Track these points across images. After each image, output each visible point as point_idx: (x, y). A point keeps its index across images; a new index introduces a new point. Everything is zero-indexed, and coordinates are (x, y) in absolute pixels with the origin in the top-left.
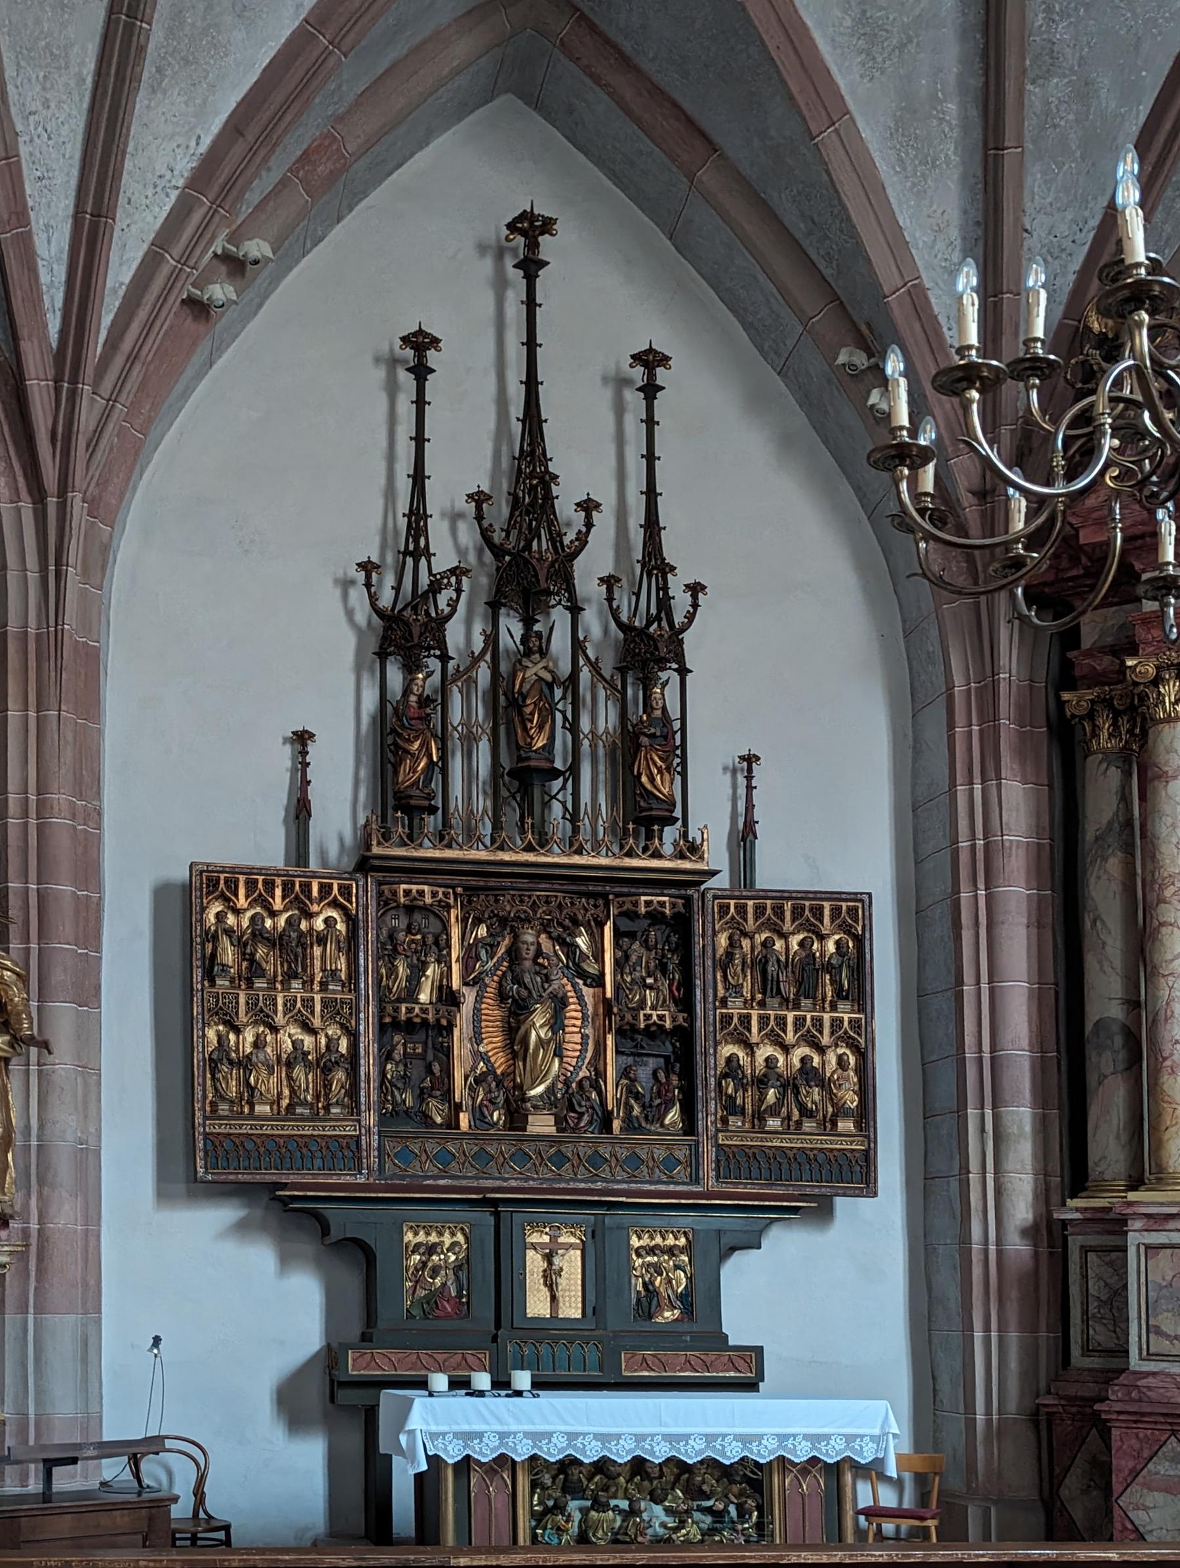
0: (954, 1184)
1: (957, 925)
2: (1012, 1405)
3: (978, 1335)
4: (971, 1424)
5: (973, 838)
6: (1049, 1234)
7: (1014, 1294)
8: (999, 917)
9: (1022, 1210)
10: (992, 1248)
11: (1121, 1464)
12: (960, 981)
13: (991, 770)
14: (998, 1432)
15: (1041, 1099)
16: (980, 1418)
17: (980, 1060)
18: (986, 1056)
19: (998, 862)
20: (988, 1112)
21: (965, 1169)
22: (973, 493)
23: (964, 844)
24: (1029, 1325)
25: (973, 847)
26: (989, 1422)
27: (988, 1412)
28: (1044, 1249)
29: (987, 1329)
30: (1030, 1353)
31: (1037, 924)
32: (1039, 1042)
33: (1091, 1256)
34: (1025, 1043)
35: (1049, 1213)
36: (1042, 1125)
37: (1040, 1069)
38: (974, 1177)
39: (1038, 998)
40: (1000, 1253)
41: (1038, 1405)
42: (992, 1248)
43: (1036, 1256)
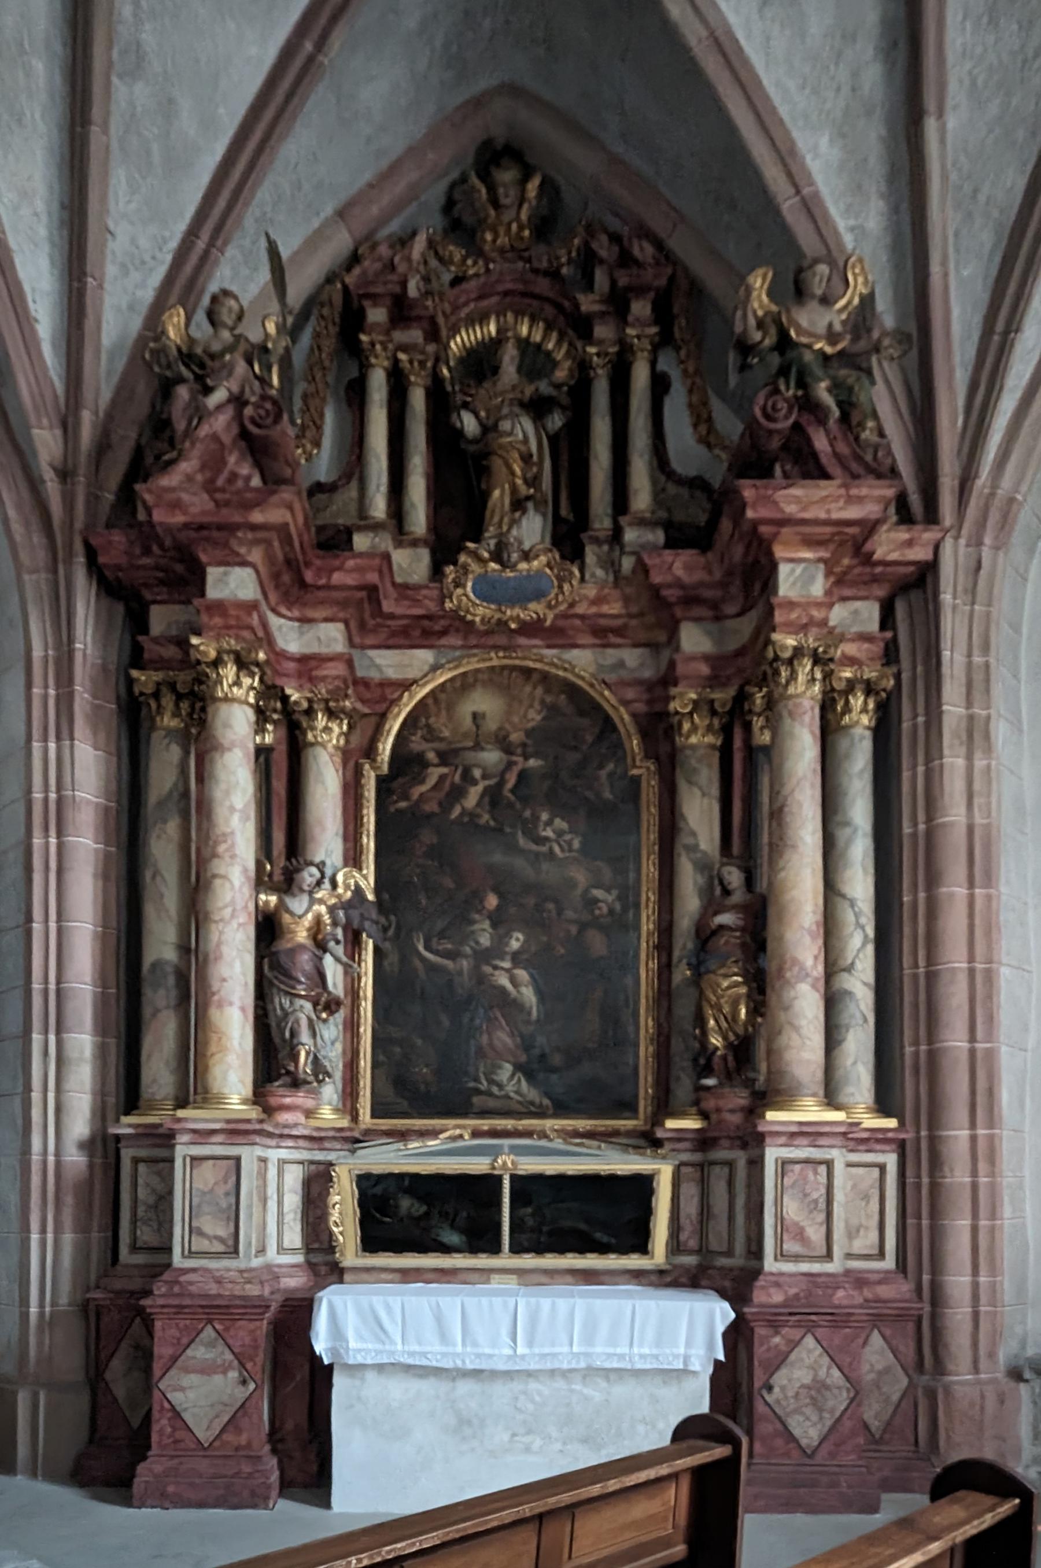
0: (17, 1101)
1: (28, 869)
2: (64, 1300)
3: (35, 1237)
4: (25, 1316)
5: (46, 789)
6: (104, 1147)
7: (69, 1200)
8: (67, 865)
9: (80, 1125)
10: (51, 1159)
11: (162, 1351)
12: (29, 919)
13: (65, 730)
14: (48, 1324)
15: (101, 1029)
16: (33, 1310)
17: (46, 992)
18: (52, 987)
19: (69, 814)
20: (52, 1038)
21: (28, 1088)
22: (55, 469)
23: (37, 796)
24: (82, 1228)
25: (46, 800)
26: (41, 1314)
27: (42, 1306)
28: (98, 1161)
29: (43, 1231)
30: (82, 1252)
31: (104, 875)
32: (102, 979)
33: (142, 1168)
34: (88, 979)
35: (104, 1128)
36: (101, 1052)
37: (102, 1004)
38: (36, 1096)
39: (102, 939)
40: (58, 1164)
41: (88, 1300)
42: (51, 1159)
43: (91, 1166)
